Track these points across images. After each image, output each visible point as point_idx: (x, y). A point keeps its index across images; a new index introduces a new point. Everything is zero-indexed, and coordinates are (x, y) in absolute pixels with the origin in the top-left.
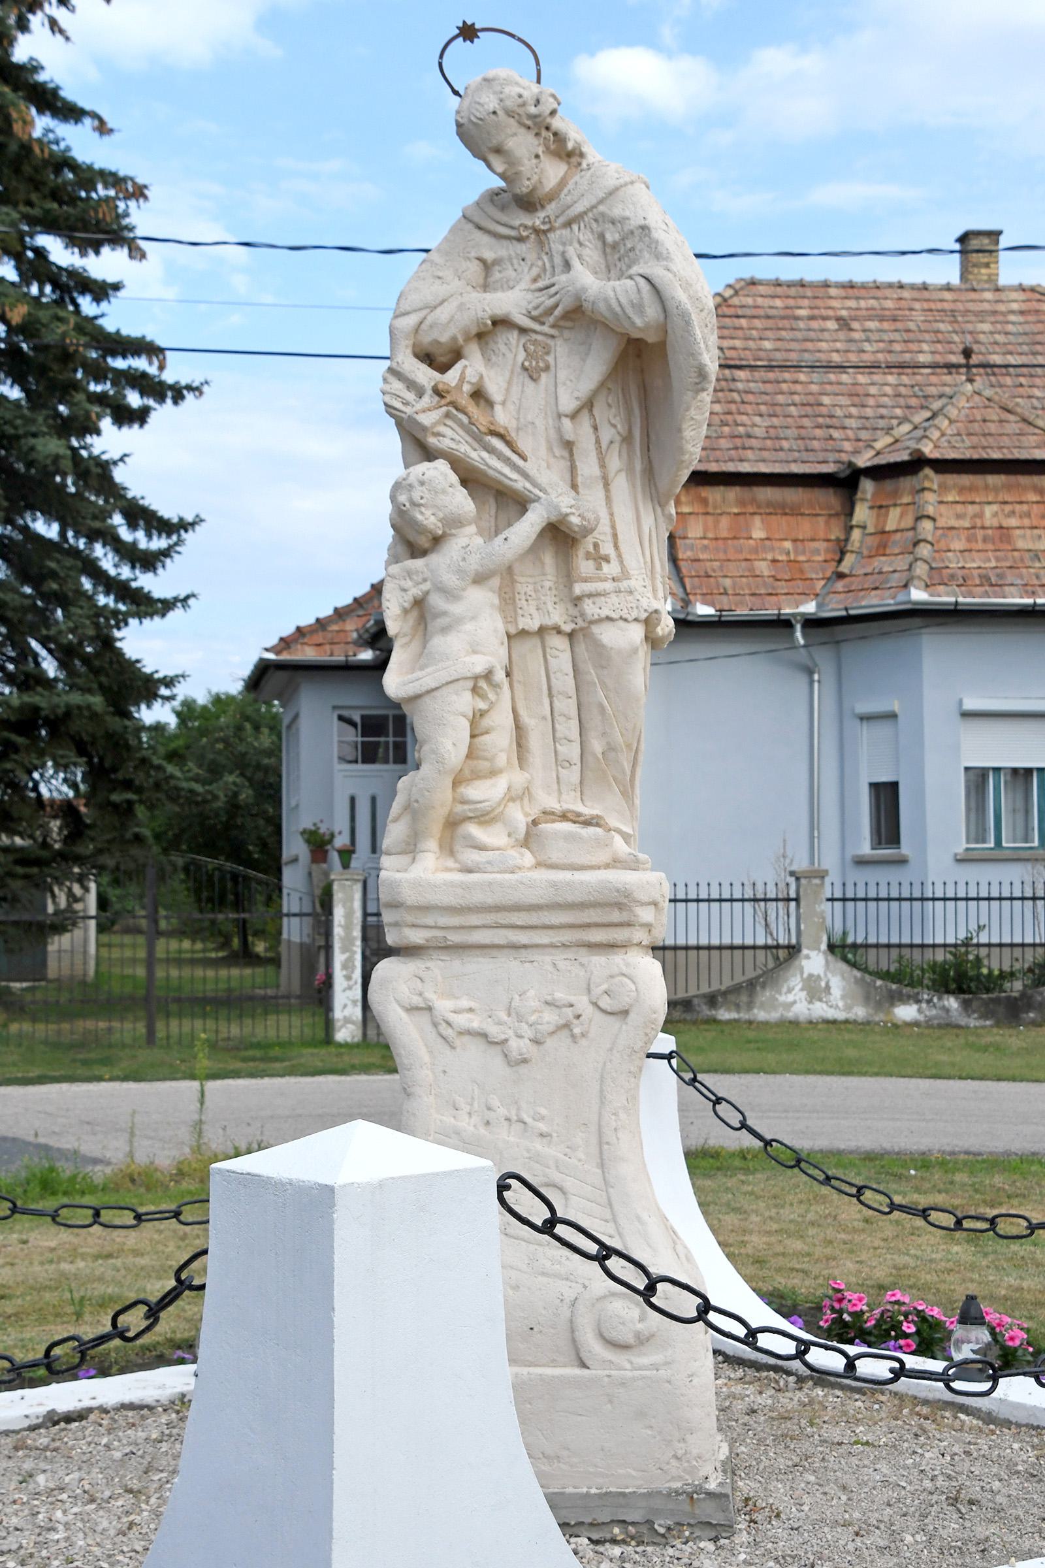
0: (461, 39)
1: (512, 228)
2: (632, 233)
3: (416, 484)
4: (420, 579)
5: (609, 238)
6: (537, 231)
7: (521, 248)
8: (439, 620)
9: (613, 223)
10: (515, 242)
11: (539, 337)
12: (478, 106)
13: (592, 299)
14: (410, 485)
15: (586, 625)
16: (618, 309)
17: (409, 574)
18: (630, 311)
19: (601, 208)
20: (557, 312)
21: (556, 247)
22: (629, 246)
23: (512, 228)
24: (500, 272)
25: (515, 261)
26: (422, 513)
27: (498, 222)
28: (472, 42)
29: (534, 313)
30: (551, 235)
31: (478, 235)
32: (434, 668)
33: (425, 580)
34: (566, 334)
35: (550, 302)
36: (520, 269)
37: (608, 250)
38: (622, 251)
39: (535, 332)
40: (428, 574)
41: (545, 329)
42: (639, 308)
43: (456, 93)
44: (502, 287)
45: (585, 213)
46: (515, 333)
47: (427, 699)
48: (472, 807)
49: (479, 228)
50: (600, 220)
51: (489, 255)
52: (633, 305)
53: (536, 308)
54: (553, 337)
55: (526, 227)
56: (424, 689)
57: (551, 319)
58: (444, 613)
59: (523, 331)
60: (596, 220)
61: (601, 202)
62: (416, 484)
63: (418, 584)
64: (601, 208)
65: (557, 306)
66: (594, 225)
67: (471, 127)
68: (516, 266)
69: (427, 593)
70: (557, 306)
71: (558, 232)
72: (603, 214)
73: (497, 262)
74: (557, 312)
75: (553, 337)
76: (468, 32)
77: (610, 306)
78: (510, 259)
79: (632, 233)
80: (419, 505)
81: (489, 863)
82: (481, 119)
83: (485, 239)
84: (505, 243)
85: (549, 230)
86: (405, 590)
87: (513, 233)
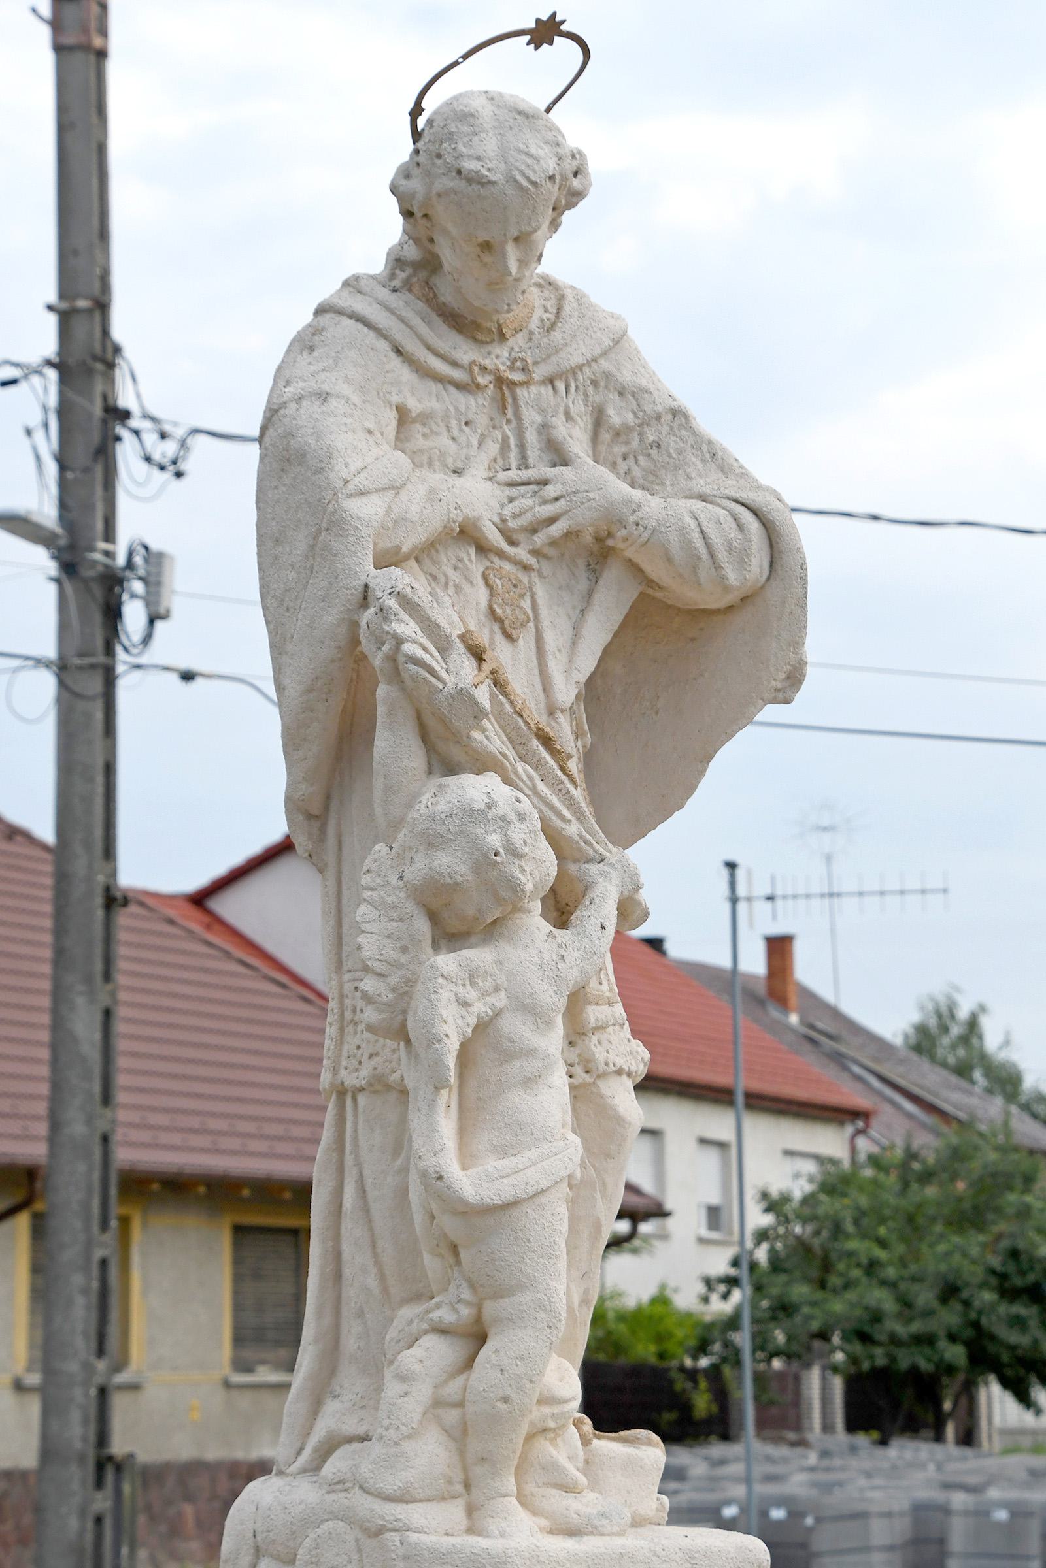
0: (528, 37)
1: (455, 364)
2: (659, 417)
3: (512, 816)
4: (488, 985)
5: (616, 416)
6: (500, 381)
7: (463, 401)
8: (517, 1063)
9: (621, 394)
10: (452, 389)
11: (507, 566)
12: (529, 161)
13: (654, 523)
14: (503, 818)
15: (588, 1079)
16: (703, 550)
17: (472, 978)
18: (722, 556)
19: (604, 364)
20: (556, 530)
21: (531, 417)
22: (651, 437)
23: (455, 364)
24: (424, 435)
25: (454, 423)
26: (523, 870)
27: (429, 348)
28: (537, 48)
29: (512, 524)
30: (521, 392)
31: (395, 362)
32: (532, 1154)
33: (497, 989)
34: (546, 568)
35: (548, 510)
36: (463, 439)
37: (606, 436)
38: (635, 444)
39: (501, 555)
40: (502, 980)
41: (521, 553)
42: (742, 558)
43: (416, 111)
44: (430, 464)
45: (580, 367)
46: (472, 551)
47: (528, 1208)
48: (556, 1409)
49: (398, 351)
50: (602, 384)
51: (414, 405)
52: (730, 549)
53: (515, 516)
54: (526, 568)
55: (484, 369)
56: (531, 1192)
57: (539, 539)
58: (532, 1052)
59: (483, 549)
60: (594, 383)
61: (604, 354)
62: (512, 816)
63: (484, 994)
64: (604, 364)
65: (552, 520)
66: (591, 390)
67: (510, 190)
68: (456, 433)
69: (498, 1014)
70: (552, 520)
71: (534, 389)
72: (608, 375)
73: (424, 418)
74: (556, 530)
75: (526, 568)
76: (545, 32)
77: (690, 541)
78: (446, 417)
79: (659, 417)
80: (521, 856)
81: (602, 1515)
82: (535, 184)
83: (406, 374)
84: (435, 387)
85: (525, 384)
86: (465, 1004)
87: (457, 375)
